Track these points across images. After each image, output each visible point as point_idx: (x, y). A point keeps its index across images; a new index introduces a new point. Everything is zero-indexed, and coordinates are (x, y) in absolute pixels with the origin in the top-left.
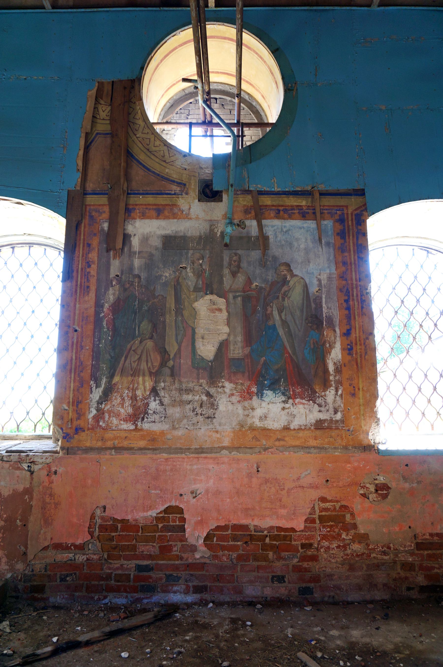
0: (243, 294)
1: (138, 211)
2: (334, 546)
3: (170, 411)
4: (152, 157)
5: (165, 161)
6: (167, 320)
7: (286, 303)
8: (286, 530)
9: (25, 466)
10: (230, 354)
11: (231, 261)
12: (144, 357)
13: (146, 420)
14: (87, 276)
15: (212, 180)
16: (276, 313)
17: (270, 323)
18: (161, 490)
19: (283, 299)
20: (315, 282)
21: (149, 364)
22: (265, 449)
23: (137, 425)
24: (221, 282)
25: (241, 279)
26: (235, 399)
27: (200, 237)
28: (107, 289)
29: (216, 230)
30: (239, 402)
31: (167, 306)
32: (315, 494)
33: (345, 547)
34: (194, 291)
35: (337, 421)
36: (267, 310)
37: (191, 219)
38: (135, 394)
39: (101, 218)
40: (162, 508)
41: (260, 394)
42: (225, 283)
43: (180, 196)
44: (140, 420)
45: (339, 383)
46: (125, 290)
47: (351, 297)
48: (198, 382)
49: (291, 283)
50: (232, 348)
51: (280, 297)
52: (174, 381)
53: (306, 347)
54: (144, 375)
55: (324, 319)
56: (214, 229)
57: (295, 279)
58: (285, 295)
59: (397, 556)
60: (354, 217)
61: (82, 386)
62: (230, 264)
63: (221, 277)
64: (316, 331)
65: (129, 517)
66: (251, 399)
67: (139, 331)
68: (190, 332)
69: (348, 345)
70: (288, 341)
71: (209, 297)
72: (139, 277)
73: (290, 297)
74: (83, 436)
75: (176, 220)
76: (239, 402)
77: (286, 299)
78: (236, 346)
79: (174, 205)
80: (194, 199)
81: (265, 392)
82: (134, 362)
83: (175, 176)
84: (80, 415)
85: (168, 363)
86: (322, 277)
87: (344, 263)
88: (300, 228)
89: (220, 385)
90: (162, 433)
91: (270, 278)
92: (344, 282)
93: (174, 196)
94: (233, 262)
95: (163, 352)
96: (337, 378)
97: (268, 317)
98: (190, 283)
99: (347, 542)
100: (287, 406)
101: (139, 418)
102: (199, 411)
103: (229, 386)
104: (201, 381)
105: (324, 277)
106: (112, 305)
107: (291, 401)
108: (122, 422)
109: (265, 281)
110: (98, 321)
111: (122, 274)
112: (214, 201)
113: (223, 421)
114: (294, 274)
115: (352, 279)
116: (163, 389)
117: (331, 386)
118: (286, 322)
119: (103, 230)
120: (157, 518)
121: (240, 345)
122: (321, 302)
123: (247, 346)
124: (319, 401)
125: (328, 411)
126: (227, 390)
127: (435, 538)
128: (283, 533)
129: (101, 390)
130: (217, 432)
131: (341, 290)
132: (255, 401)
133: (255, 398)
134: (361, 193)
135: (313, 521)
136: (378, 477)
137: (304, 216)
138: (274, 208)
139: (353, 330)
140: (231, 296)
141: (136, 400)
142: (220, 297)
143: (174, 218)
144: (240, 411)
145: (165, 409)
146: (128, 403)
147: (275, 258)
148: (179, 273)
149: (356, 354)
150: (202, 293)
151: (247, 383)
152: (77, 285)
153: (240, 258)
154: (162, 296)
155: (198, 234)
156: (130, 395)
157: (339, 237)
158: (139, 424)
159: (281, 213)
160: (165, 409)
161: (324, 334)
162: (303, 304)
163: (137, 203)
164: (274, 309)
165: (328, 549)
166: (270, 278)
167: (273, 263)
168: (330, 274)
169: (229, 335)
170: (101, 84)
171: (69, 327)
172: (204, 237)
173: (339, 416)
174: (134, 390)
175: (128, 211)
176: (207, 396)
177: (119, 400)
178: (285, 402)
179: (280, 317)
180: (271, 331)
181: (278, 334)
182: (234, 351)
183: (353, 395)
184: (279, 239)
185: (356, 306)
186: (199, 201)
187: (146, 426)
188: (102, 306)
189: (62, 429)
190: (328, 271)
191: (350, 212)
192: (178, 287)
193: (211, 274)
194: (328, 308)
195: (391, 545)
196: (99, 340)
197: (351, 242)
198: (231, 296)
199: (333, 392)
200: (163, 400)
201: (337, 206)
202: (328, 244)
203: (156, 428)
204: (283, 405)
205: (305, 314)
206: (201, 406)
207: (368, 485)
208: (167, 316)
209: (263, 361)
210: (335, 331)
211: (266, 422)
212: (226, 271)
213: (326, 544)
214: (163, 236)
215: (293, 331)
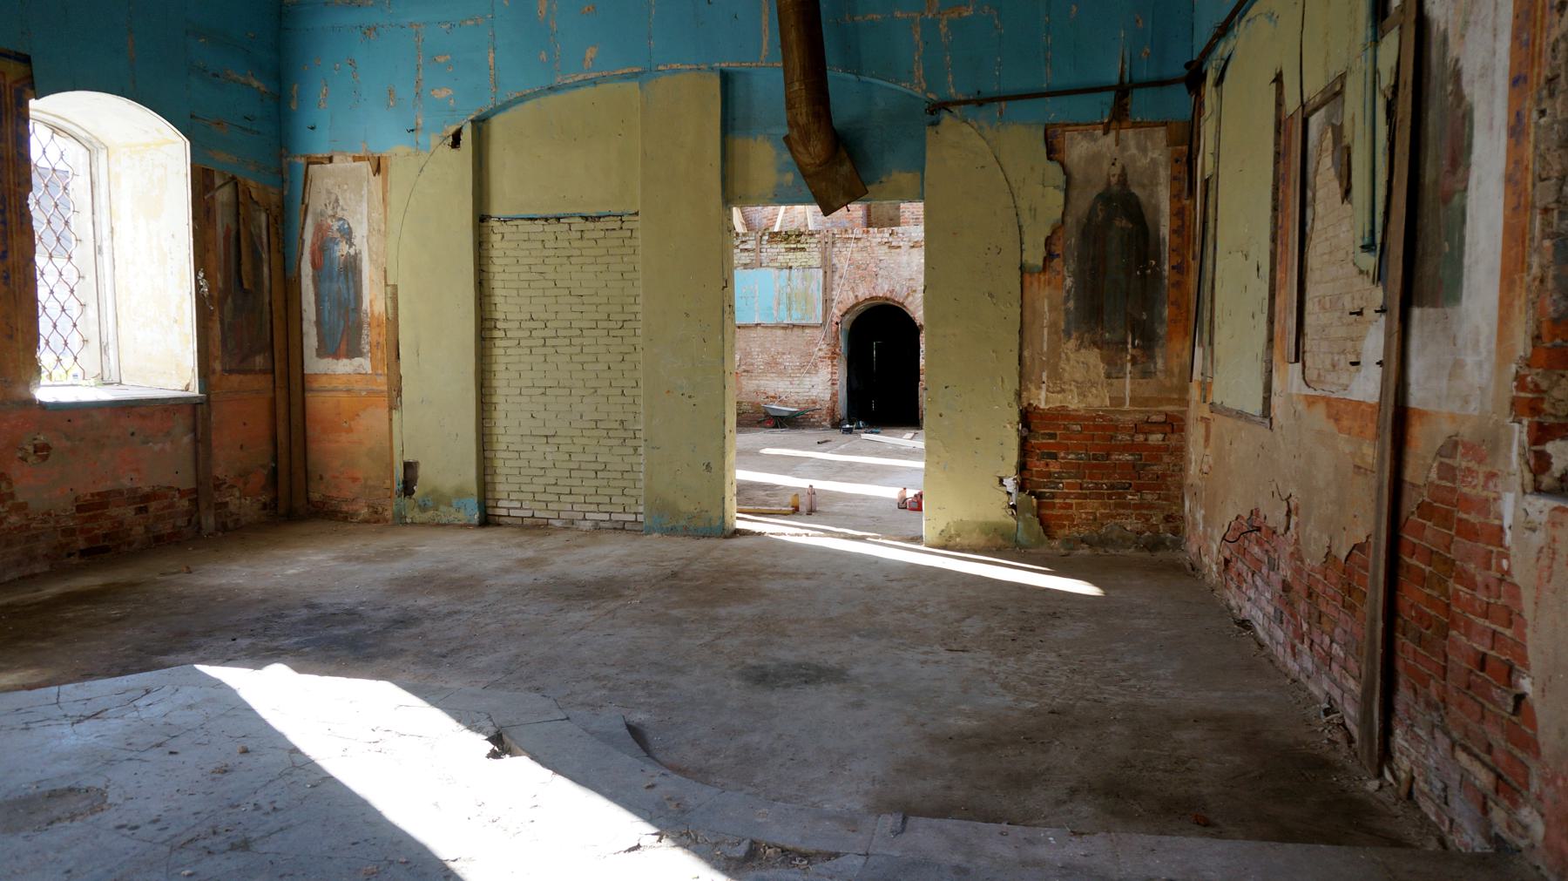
47: (7, 207)
59: (57, 522)
69: (4, 271)
127: (97, 498)
136: (38, 437)
139: (10, 254)
149: (14, 284)
185: (14, 219)
191: (8, 84)
195: (52, 512)
207: (26, 447)
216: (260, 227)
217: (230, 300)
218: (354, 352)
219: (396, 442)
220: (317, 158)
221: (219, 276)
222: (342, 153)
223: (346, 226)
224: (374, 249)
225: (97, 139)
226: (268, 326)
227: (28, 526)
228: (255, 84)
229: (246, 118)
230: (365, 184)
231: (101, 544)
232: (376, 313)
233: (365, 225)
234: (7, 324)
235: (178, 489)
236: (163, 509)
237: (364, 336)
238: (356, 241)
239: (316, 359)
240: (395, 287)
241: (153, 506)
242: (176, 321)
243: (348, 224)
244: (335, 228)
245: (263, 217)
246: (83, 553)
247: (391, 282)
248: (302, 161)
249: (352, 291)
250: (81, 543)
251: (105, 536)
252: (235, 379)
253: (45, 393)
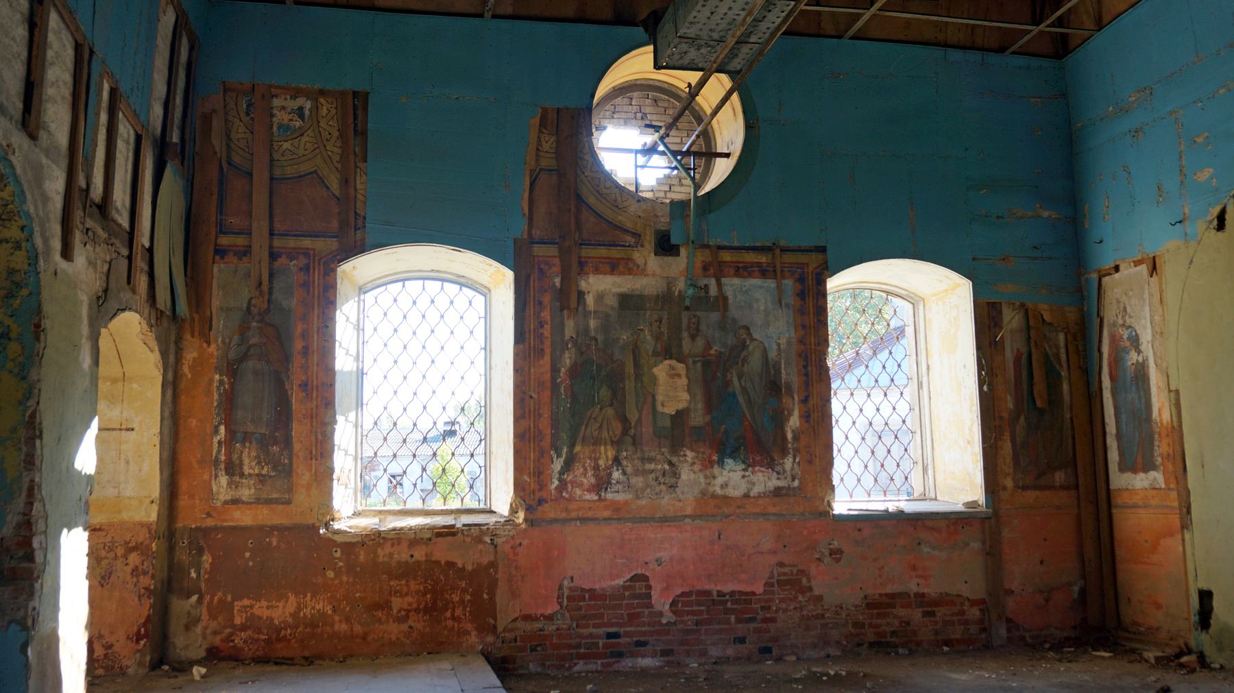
2: (792, 607)
3: (634, 480)
4: (603, 200)
5: (617, 207)
6: (627, 387)
7: (745, 369)
8: (747, 594)
9: (488, 539)
12: (605, 426)
13: (609, 490)
14: (540, 337)
15: (669, 231)
16: (735, 380)
17: (730, 390)
18: (627, 559)
19: (743, 365)
20: (775, 347)
21: (611, 433)
22: (727, 516)
23: (600, 495)
24: (680, 346)
25: (700, 342)
26: (696, 468)
27: (658, 296)
28: (562, 353)
29: (674, 288)
30: (701, 470)
31: (627, 370)
32: (774, 560)
33: (801, 608)
34: (652, 356)
35: (794, 488)
37: (647, 275)
38: (598, 464)
39: (551, 271)
40: (629, 577)
41: (721, 463)
44: (603, 490)
45: (797, 451)
46: (582, 353)
48: (660, 451)
49: (751, 348)
50: (693, 415)
52: (636, 451)
54: (605, 444)
58: (745, 360)
60: (814, 276)
61: (543, 456)
62: (689, 327)
63: (680, 340)
65: (597, 587)
66: (712, 467)
68: (650, 399)
71: (667, 362)
72: (596, 339)
74: (546, 507)
75: (631, 277)
76: (701, 470)
79: (629, 259)
80: (650, 252)
81: (726, 460)
82: (595, 430)
83: (629, 225)
84: (542, 486)
86: (781, 342)
87: (804, 327)
88: (760, 287)
89: (682, 453)
90: (626, 503)
91: (729, 342)
92: (803, 347)
93: (628, 248)
94: (692, 325)
95: (624, 420)
96: (795, 446)
97: (728, 383)
98: (648, 347)
99: (804, 603)
100: (747, 474)
101: (602, 488)
102: (662, 481)
103: (690, 455)
104: (663, 450)
105: (783, 341)
107: (750, 469)
108: (586, 493)
110: (555, 387)
111: (577, 336)
112: (670, 255)
113: (686, 489)
115: (810, 344)
116: (625, 458)
117: (790, 453)
119: (554, 285)
120: (625, 588)
121: (700, 412)
122: (780, 368)
124: (778, 468)
125: (786, 478)
126: (689, 459)
128: (743, 597)
129: (562, 460)
130: (680, 501)
131: (800, 355)
132: (716, 470)
133: (716, 466)
134: (822, 250)
135: (772, 585)
137: (764, 274)
138: (732, 264)
140: (690, 361)
141: (599, 470)
142: (680, 361)
144: (702, 480)
145: (628, 479)
146: (590, 473)
147: (734, 321)
149: (814, 421)
151: (708, 451)
152: (530, 347)
153: (699, 321)
155: (655, 293)
156: (593, 464)
157: (798, 299)
158: (603, 494)
159: (741, 270)
160: (628, 479)
163: (590, 255)
165: (785, 611)
166: (729, 342)
168: (790, 338)
169: (690, 402)
170: (545, 111)
171: (524, 393)
173: (796, 483)
174: (596, 460)
175: (582, 264)
176: (669, 465)
177: (581, 470)
178: (744, 470)
179: (740, 384)
181: (738, 401)
182: (694, 418)
183: (810, 462)
184: (738, 299)
186: (655, 255)
187: (610, 496)
188: (559, 371)
189: (524, 501)
190: (787, 335)
191: (810, 271)
196: (557, 408)
197: (811, 303)
198: (690, 361)
199: (791, 460)
200: (625, 469)
201: (797, 263)
202: (788, 306)
203: (620, 497)
204: (743, 473)
206: (664, 475)
208: (627, 382)
210: (793, 398)
211: (727, 490)
212: (685, 335)
213: (784, 605)
215: (752, 398)
216: (1057, 347)
217: (1022, 419)
218: (1148, 466)
219: (1190, 566)
220: (1106, 270)
221: (1008, 397)
222: (1123, 259)
223: (1134, 334)
224: (1158, 354)
225: (913, 293)
226: (1070, 441)
227: (823, 616)
228: (1046, 214)
229: (1034, 247)
230: (1146, 286)
231: (889, 639)
232: (1165, 422)
233: (1149, 331)
234: (808, 452)
235: (968, 598)
236: (953, 614)
237: (1156, 448)
238: (1143, 348)
239: (1119, 473)
240: (1177, 392)
241: (941, 612)
242: (969, 443)
243: (1136, 331)
244: (1125, 337)
245: (1061, 337)
246: (872, 645)
247: (1173, 388)
248: (1095, 276)
249: (1143, 401)
250: (871, 637)
251: (893, 633)
252: (1031, 495)
253: (840, 507)
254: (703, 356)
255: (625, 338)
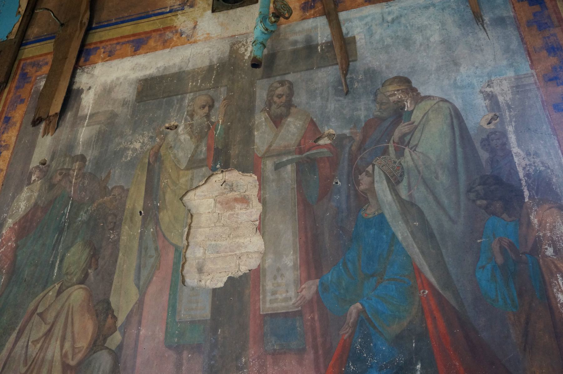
0: (298, 156)
1: (102, 50)
6: (124, 238)
7: (408, 159)
10: (264, 302)
11: (272, 96)
17: (370, 212)
19: (400, 153)
20: (481, 102)
21: (67, 345)
24: (249, 140)
27: (211, 68)
28: (19, 190)
29: (243, 49)
31: (129, 205)
34: (187, 168)
36: (358, 183)
39: (39, 73)
42: (257, 141)
43: (180, 12)
46: (52, 187)
49: (417, 116)
51: (391, 150)
53: (480, 264)
55: (524, 183)
56: (238, 49)
57: (425, 106)
62: (269, 103)
64: (505, 216)
67: (60, 268)
68: (171, 256)
70: (423, 253)
71: (219, 177)
72: (83, 158)
73: (416, 146)
75: (167, 50)
77: (407, 150)
78: (279, 280)
80: (205, 10)
85: (109, 340)
86: (496, 89)
91: (362, 114)
94: (275, 99)
98: (181, 154)
106: (20, 221)
109: (353, 121)
111: (52, 159)
114: (422, 95)
118: (413, 204)
121: (290, 276)
123: (309, 278)
140: (269, 164)
142: (244, 170)
143: (164, 47)
148: (161, 139)
150: (204, 169)
154: (122, 187)
155: (207, 63)
161: (529, 223)
162: (455, 155)
163: (103, 39)
164: (377, 178)
167: (369, 82)
168: (518, 78)
169: (264, 255)
172: (218, 67)
180: (372, 231)
181: (394, 236)
182: (274, 293)
184: (377, 37)
186: (213, 11)
190: (511, 74)
192: (156, 165)
193: (227, 130)
194: (528, 154)
198: (269, 164)
202: (500, 22)
205: (462, 177)
208: (125, 228)
209: (354, 315)
214: (140, 81)
215: (434, 225)
254: (301, 152)
255: (138, 145)
